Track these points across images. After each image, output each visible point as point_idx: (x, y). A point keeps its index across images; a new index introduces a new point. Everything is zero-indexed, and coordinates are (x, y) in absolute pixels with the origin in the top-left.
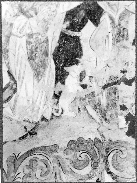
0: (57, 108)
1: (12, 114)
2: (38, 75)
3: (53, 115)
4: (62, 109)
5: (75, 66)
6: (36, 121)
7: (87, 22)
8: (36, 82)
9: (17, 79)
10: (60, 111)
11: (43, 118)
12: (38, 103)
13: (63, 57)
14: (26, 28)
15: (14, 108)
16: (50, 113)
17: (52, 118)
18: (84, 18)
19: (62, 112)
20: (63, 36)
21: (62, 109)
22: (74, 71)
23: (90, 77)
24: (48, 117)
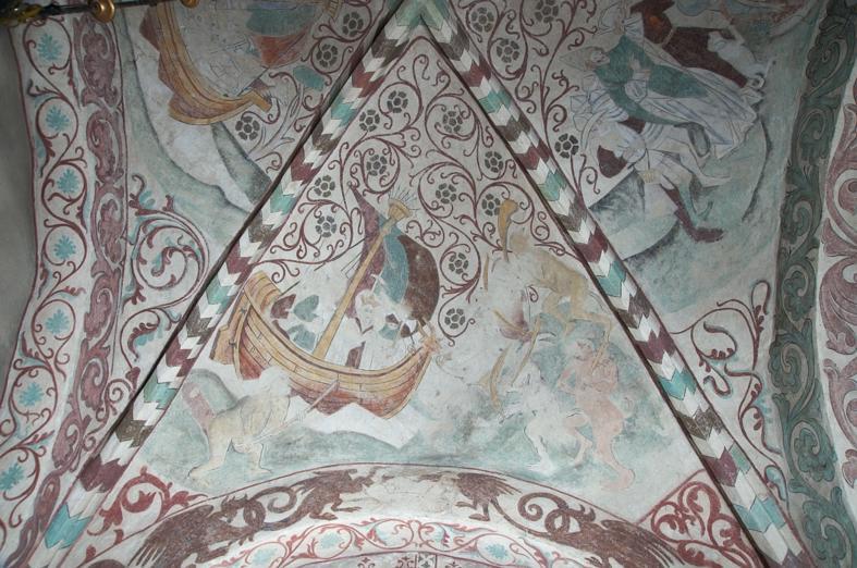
0: (752, 81)
1: (727, 146)
2: (697, 91)
3: (758, 90)
4: (757, 74)
5: (710, 41)
6: (755, 117)
7: (665, 15)
8: (706, 99)
9: (690, 120)
10: (759, 78)
11: (756, 107)
12: (732, 106)
13: (692, 55)
14: (640, 85)
15: (721, 138)
16: (754, 93)
17: (763, 94)
18: (659, 18)
19: (761, 75)
20: (667, 48)
21: (757, 74)
22: (715, 43)
23: (732, 23)
24: (758, 98)
